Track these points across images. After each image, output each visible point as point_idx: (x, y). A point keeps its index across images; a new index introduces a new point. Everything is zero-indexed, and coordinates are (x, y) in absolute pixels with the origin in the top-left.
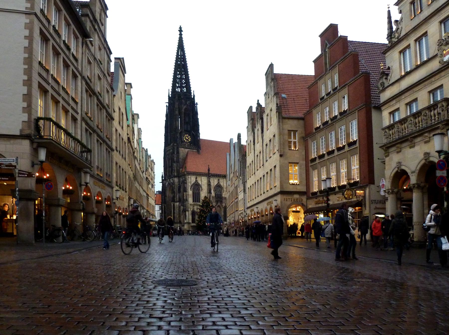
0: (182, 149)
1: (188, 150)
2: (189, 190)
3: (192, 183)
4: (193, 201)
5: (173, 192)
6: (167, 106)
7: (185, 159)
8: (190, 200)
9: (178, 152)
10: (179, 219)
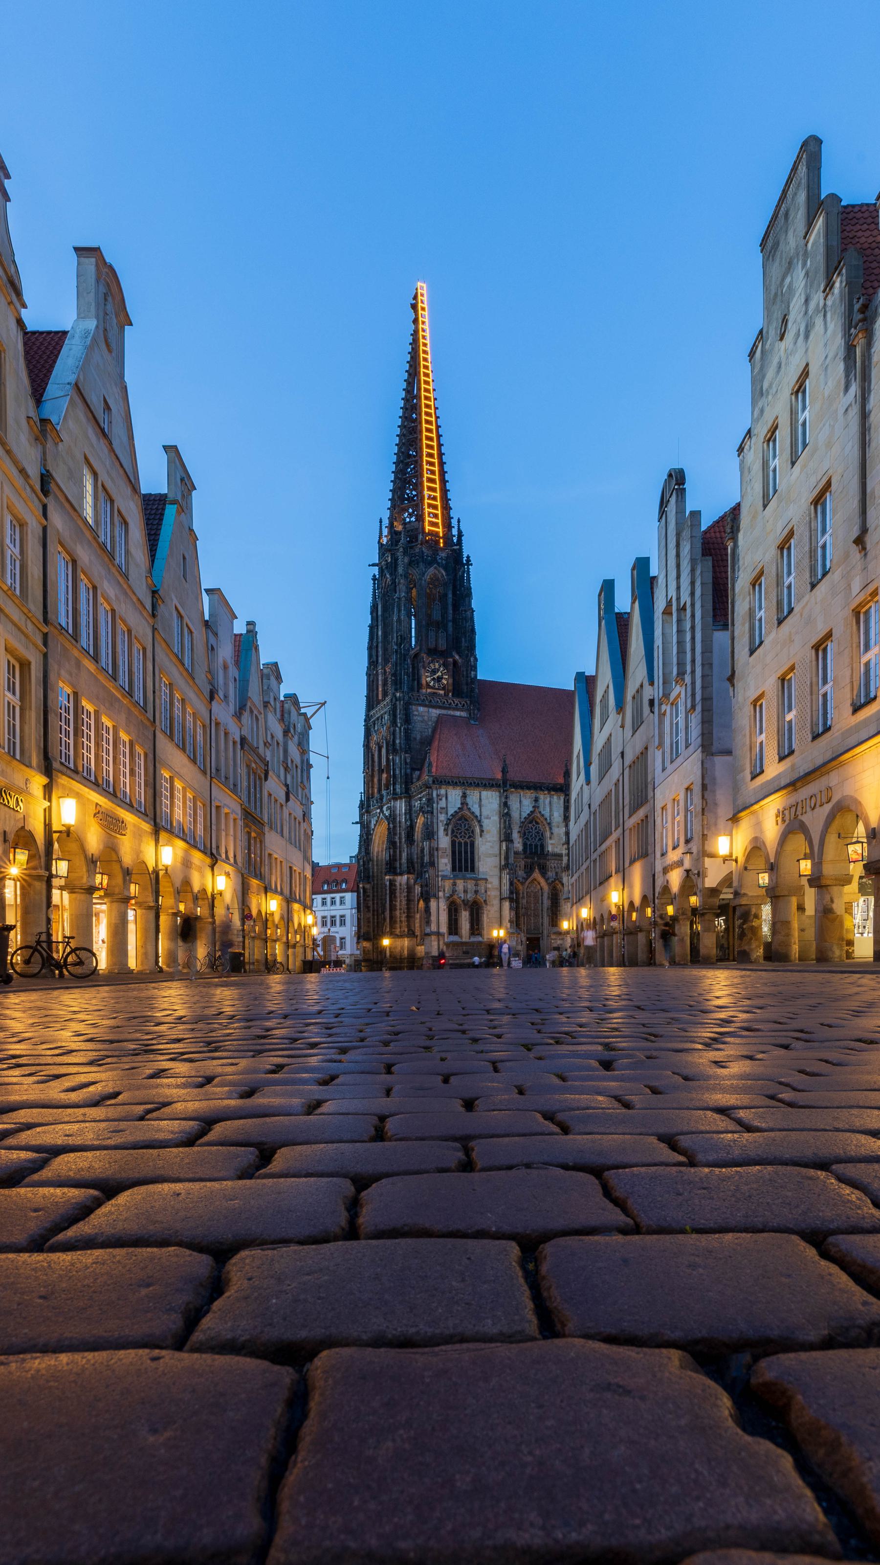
0: (421, 709)
1: (438, 711)
2: (441, 832)
3: (451, 811)
4: (454, 869)
5: (392, 843)
6: (374, 579)
7: (428, 742)
8: (444, 864)
9: (407, 720)
10: (409, 926)
